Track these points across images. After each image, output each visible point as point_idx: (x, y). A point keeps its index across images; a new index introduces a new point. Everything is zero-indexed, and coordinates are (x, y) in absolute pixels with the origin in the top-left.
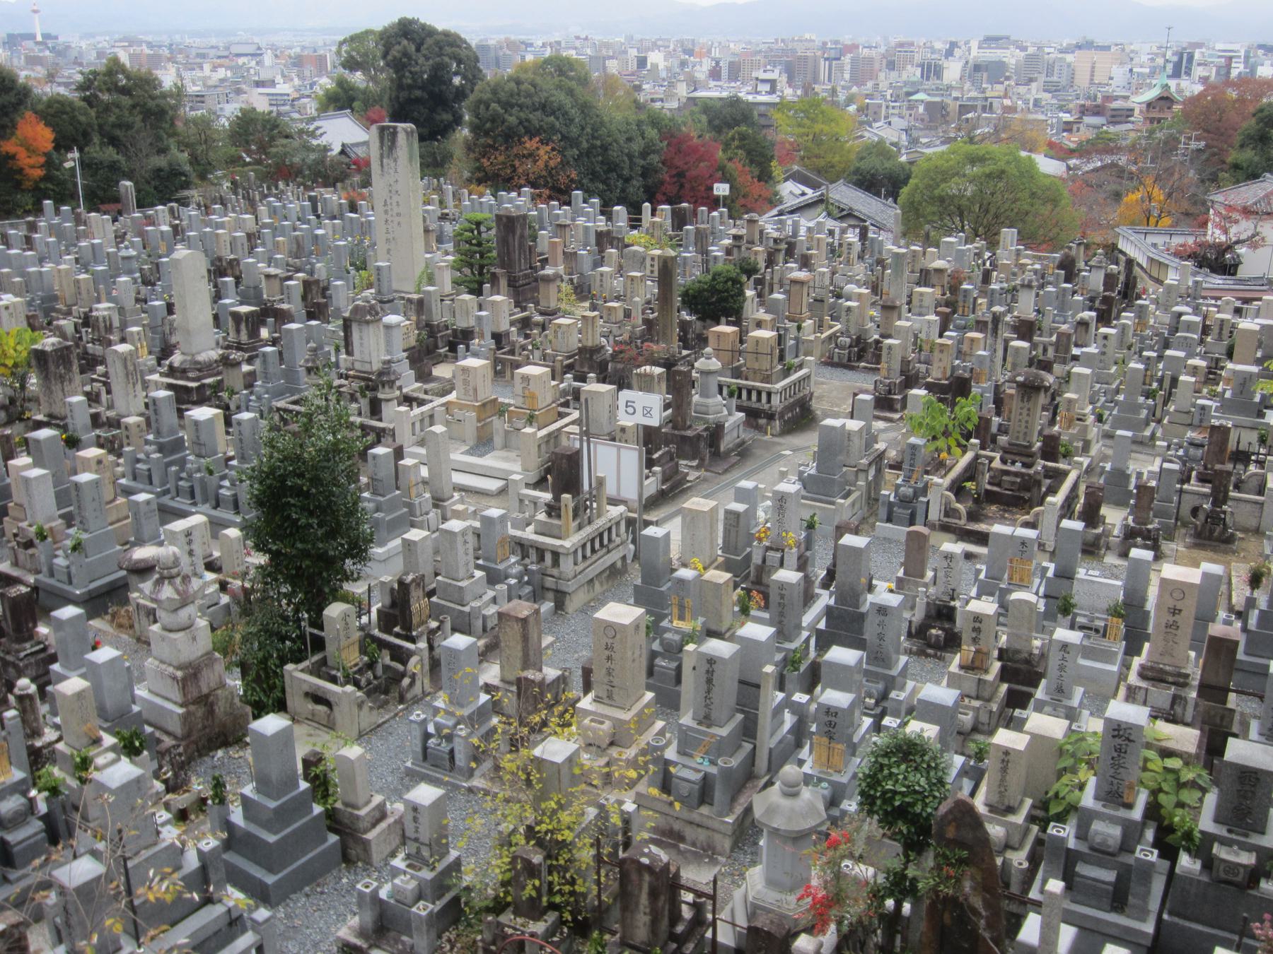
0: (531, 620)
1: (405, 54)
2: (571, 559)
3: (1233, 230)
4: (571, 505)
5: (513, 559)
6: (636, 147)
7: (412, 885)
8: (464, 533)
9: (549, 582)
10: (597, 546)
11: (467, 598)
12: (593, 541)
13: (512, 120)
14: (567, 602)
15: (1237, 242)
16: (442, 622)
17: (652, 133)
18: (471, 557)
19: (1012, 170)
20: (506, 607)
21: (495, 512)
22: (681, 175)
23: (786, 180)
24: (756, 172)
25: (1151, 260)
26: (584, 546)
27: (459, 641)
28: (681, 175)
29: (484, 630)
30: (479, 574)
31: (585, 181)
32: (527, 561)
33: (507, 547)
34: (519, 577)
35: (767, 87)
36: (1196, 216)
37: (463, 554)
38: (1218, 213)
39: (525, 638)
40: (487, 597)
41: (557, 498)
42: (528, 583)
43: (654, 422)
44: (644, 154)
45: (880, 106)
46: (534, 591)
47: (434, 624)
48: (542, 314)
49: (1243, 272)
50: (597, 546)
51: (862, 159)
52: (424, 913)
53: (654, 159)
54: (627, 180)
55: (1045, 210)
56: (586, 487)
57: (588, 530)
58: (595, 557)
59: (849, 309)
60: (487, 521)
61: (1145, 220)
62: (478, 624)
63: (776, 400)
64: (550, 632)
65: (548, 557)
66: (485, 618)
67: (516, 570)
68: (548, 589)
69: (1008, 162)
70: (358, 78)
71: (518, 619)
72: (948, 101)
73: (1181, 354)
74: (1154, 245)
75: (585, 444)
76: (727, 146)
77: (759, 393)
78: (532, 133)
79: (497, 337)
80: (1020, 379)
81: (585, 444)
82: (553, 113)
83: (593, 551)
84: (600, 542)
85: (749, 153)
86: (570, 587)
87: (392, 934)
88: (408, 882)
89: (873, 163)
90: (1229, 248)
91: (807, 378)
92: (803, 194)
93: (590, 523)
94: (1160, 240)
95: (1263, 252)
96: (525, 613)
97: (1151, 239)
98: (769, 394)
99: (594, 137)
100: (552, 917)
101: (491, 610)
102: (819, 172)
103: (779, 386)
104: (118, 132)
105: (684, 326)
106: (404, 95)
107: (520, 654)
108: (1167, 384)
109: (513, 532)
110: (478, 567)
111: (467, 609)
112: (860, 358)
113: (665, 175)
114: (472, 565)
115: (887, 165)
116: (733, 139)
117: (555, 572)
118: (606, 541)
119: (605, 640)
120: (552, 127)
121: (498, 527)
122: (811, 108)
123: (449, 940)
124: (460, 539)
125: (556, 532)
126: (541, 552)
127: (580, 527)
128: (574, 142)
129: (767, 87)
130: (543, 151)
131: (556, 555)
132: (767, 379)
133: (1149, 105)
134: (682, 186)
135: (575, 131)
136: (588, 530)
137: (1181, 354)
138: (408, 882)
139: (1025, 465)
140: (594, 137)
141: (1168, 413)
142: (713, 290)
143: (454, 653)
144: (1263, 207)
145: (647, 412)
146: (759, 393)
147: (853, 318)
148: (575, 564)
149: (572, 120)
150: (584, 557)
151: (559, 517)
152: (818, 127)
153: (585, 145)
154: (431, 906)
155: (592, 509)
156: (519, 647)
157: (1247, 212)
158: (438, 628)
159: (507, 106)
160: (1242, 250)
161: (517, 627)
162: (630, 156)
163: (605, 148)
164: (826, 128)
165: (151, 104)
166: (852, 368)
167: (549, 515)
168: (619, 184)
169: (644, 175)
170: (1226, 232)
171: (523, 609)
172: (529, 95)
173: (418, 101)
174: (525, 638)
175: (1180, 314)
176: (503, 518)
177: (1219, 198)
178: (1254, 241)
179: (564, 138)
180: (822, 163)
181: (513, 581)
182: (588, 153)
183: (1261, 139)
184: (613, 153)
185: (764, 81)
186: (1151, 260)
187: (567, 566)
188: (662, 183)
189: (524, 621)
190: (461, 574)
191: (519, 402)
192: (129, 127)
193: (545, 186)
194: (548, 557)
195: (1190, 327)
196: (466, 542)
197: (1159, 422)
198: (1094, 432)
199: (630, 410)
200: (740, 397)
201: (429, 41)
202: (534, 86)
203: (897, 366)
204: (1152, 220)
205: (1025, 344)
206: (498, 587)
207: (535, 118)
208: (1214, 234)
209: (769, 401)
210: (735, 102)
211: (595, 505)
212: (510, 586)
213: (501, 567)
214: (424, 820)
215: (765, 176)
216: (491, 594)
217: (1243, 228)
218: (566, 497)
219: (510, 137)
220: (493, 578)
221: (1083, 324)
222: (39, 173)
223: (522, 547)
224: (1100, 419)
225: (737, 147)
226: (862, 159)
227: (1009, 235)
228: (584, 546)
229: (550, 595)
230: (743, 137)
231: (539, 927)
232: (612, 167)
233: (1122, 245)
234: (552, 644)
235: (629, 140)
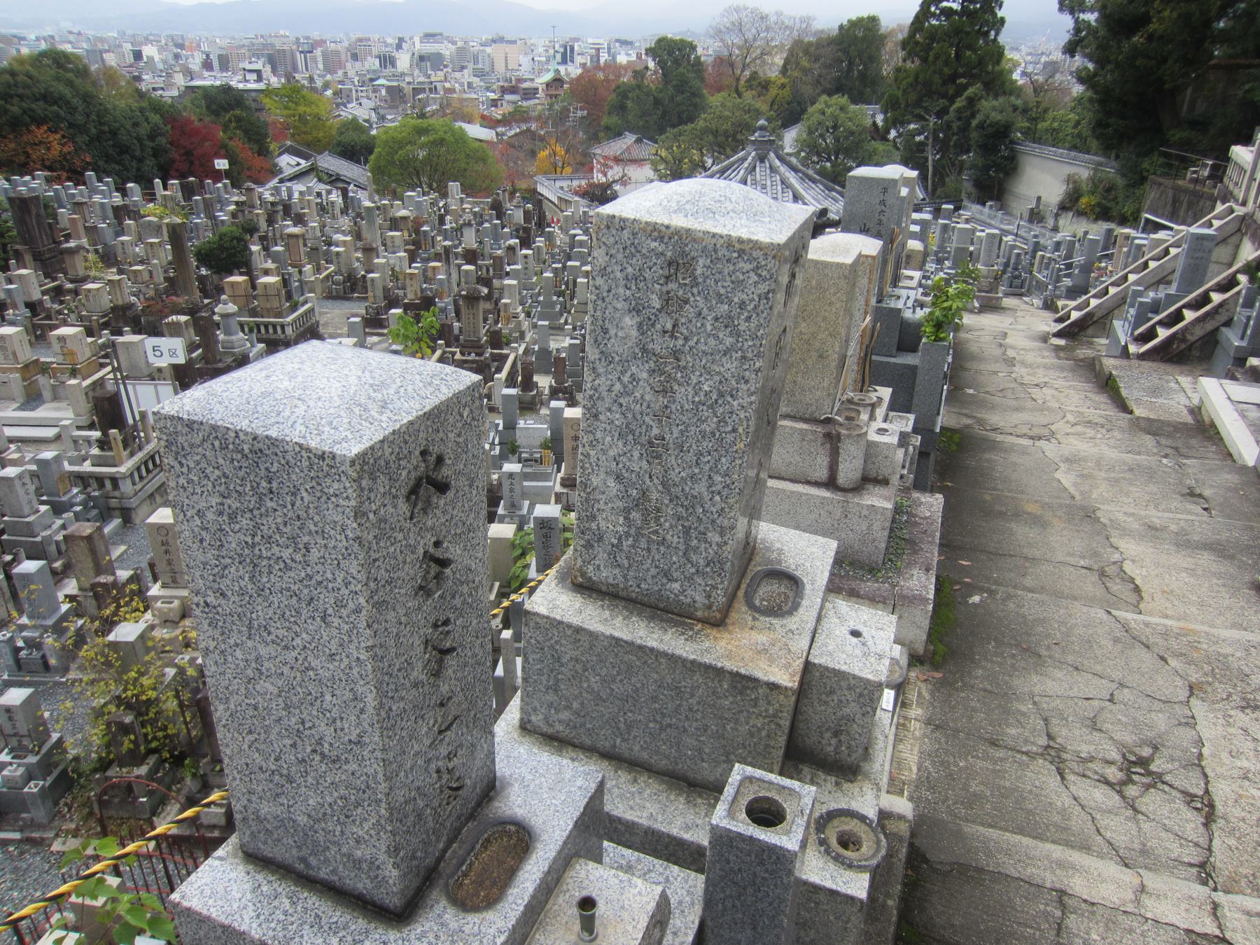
0: (96, 536)
2: (129, 481)
3: (610, 174)
4: (120, 438)
5: (75, 491)
6: (144, 130)
7: (21, 770)
8: (20, 476)
9: (114, 503)
10: (151, 466)
11: (37, 530)
12: (146, 463)
13: (15, 109)
14: (133, 516)
15: (614, 182)
16: (15, 555)
17: (155, 118)
18: (33, 496)
19: (449, 137)
20: (74, 528)
21: (48, 454)
22: (188, 153)
23: (280, 155)
24: (256, 147)
25: (560, 199)
26: (138, 469)
27: (29, 566)
29: (60, 552)
30: (43, 508)
31: (101, 163)
32: (89, 489)
33: (67, 481)
34: (84, 504)
35: (254, 76)
36: (584, 165)
37: (24, 494)
38: (598, 162)
39: (93, 552)
40: (55, 527)
41: (105, 434)
42: (93, 507)
43: (181, 360)
44: (152, 137)
46: (101, 513)
47: (8, 558)
48: (72, 282)
50: (151, 466)
51: (342, 133)
52: (35, 790)
53: (162, 141)
54: (140, 160)
55: (479, 167)
56: (130, 421)
57: (140, 456)
58: (151, 476)
59: (338, 254)
60: (43, 464)
61: (553, 170)
62: (53, 548)
63: (289, 331)
64: (123, 542)
65: (108, 484)
66: (57, 543)
67: (81, 497)
68: (114, 509)
69: (445, 132)
71: (82, 538)
72: (403, 85)
73: (578, 264)
74: (562, 188)
75: (122, 387)
76: (226, 128)
77: (274, 327)
78: (40, 122)
79: (32, 306)
80: (464, 293)
81: (122, 387)
82: (55, 103)
83: (148, 471)
84: (151, 464)
85: (246, 132)
86: (133, 503)
87: (11, 816)
88: (15, 770)
89: (350, 137)
90: (609, 186)
91: (312, 310)
92: (298, 164)
93: (140, 449)
94: (565, 184)
96: (89, 531)
97: (558, 184)
98: (283, 327)
99: (101, 124)
100: (152, 760)
101: (60, 537)
102: (308, 145)
103: (290, 319)
105: (201, 279)
107: (91, 565)
108: (571, 286)
109: (67, 467)
110: (43, 503)
111: (39, 539)
112: (353, 290)
113: (174, 154)
114: (35, 502)
115: (364, 137)
116: (230, 121)
117: (117, 494)
118: (158, 462)
119: (160, 538)
120: (58, 115)
121: (54, 467)
122: (293, 94)
123: (66, 804)
124: (17, 482)
125: (111, 462)
126: (100, 480)
127: (132, 454)
129: (254, 76)
131: (115, 480)
132: (279, 315)
133: (548, 85)
134: (192, 163)
135: (80, 119)
136: (140, 456)
137: (578, 264)
138: (15, 770)
139: (477, 354)
140: (101, 124)
141: (573, 305)
142: (221, 248)
143: (26, 577)
144: (626, 156)
145: (173, 353)
146: (274, 327)
147: (342, 259)
148: (134, 484)
149: (75, 109)
150: (141, 478)
151: (111, 449)
152: (302, 109)
153: (94, 131)
154: (41, 783)
155: (140, 438)
156: (89, 560)
157: (617, 160)
158: (13, 560)
160: (617, 187)
161: (83, 544)
162: (139, 139)
163: (114, 133)
164: (308, 110)
166: (348, 299)
167: (102, 448)
168: (134, 164)
169: (155, 156)
170: (605, 175)
171: (87, 529)
172: (27, 87)
174: (93, 552)
175: (575, 236)
176: (57, 459)
177: (598, 151)
179: (71, 125)
180: (310, 138)
181: (78, 508)
182: (98, 138)
183: (621, 108)
184: (123, 137)
186: (560, 199)
187: (126, 487)
188: (174, 161)
189: (89, 538)
190: (26, 510)
191: (60, 359)
193: (63, 168)
194: (108, 484)
195: (581, 244)
196: (24, 484)
197: (569, 312)
198: (526, 325)
199: (158, 353)
200: (259, 331)
202: (30, 77)
203: (380, 293)
204: (559, 170)
205: (472, 268)
206: (65, 515)
207: (39, 107)
208: (599, 178)
209: (283, 332)
210: (227, 89)
211: (142, 434)
212: (76, 513)
213: (64, 499)
214: (19, 717)
215: (263, 152)
216: (59, 522)
217: (615, 172)
218: (113, 431)
220: (58, 509)
221: (511, 249)
223: (82, 480)
224: (528, 315)
225: (236, 128)
226: (342, 133)
227: (454, 187)
228: (138, 469)
229: (117, 513)
230: (239, 120)
231: (143, 770)
232: (124, 150)
233: (540, 189)
234: (125, 551)
235: (136, 125)
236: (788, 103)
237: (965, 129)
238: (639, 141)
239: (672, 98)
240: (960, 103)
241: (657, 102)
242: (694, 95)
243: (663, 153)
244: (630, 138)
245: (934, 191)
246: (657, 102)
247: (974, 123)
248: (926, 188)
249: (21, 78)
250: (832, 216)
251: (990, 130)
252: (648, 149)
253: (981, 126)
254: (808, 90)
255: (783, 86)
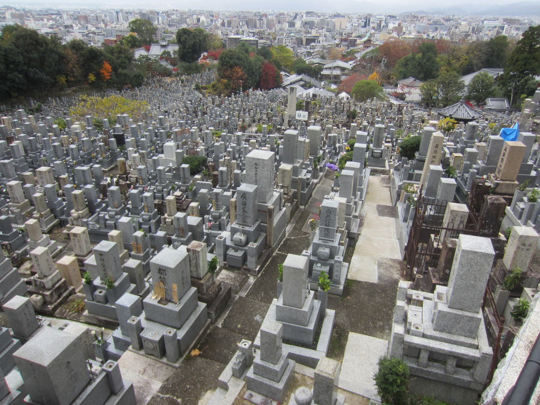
1: (186, 39)
22: (267, 74)
28: (267, 74)
35: (252, 35)
45: (283, 39)
49: (406, 99)
53: (261, 70)
70: (135, 34)
72: (302, 37)
78: (237, 65)
85: (277, 65)
95: (411, 96)
104: (123, 65)
106: (185, 50)
113: (263, 74)
128: (245, 68)
130: (239, 70)
133: (365, 42)
152: (285, 55)
157: (408, 86)
159: (230, 58)
160: (407, 95)
162: (257, 70)
163: (252, 68)
165: (129, 56)
173: (190, 52)
178: (409, 93)
184: (254, 70)
185: (251, 33)
192: (125, 63)
195: (416, 118)
201: (191, 35)
207: (237, 61)
208: (399, 91)
217: (406, 90)
219: (231, 67)
222: (109, 77)
232: (253, 73)
235: (256, 65)
236: (467, 65)
237: (523, 88)
238: (415, 80)
239: (425, 64)
240: (523, 81)
241: (420, 64)
242: (433, 62)
243: (425, 87)
244: (411, 80)
245: (513, 103)
246: (420, 64)
247: (526, 87)
248: (509, 103)
249: (234, 53)
250: (475, 118)
251: (530, 90)
252: (421, 84)
253: (528, 89)
254: (475, 61)
255: (466, 59)
